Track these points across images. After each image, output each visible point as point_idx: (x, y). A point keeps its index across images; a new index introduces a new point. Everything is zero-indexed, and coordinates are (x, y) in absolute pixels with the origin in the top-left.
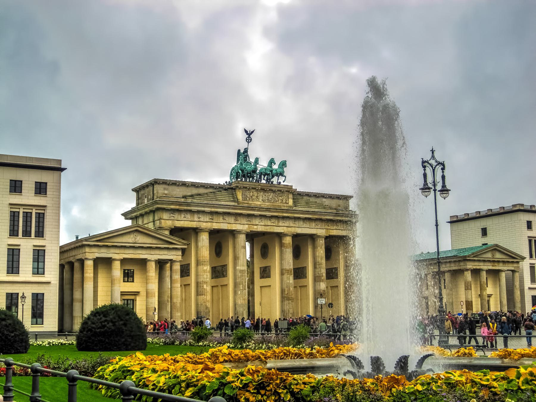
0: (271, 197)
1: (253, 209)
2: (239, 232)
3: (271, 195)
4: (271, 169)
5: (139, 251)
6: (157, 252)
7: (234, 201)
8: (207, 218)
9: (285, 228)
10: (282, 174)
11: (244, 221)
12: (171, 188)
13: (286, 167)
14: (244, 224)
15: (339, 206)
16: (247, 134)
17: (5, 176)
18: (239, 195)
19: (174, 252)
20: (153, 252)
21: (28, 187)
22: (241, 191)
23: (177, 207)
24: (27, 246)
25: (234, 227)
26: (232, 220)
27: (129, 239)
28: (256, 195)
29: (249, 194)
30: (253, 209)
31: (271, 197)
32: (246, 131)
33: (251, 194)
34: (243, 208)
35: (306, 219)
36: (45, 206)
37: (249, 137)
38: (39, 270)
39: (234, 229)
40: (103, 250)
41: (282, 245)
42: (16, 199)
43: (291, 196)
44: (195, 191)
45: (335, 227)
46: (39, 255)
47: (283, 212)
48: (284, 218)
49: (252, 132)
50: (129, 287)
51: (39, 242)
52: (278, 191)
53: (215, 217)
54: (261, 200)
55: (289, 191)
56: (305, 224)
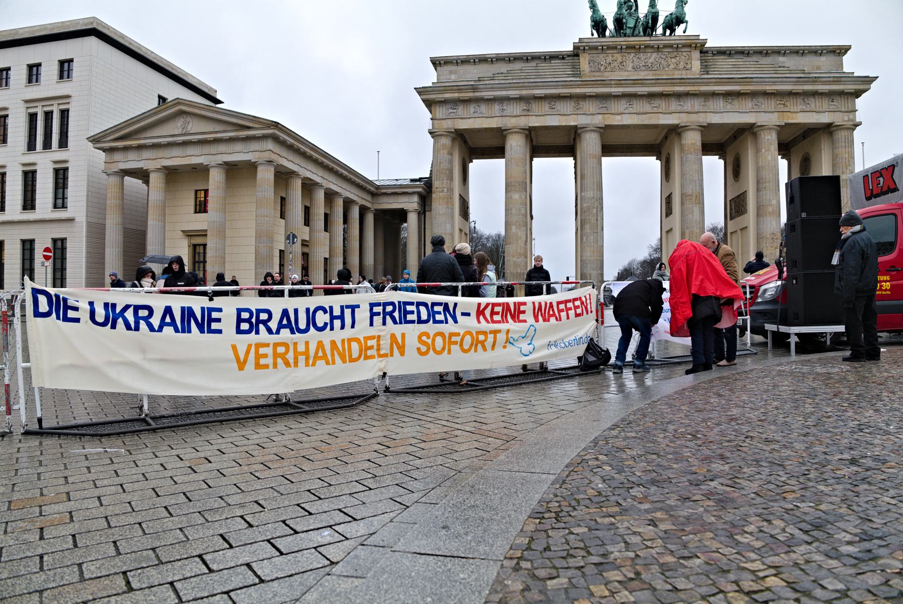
0: (652, 60)
1: (603, 83)
3: (652, 57)
4: (653, 11)
5: (191, 150)
6: (222, 148)
7: (574, 75)
8: (516, 109)
9: (684, 115)
11: (590, 106)
12: (462, 69)
14: (593, 115)
15: (818, 68)
17: (16, 61)
18: (584, 61)
19: (255, 146)
20: (213, 149)
21: (49, 71)
22: (586, 55)
23: (456, 95)
26: (566, 107)
27: (174, 129)
28: (620, 60)
29: (601, 58)
31: (652, 60)
33: (610, 59)
35: (728, 95)
36: (68, 97)
38: (60, 201)
40: (132, 155)
41: (682, 147)
43: (696, 55)
44: (504, 68)
45: (800, 108)
46: (61, 176)
47: (673, 84)
48: (679, 96)
51: (61, 155)
52: (665, 46)
53: (535, 107)
54: (630, 68)
55: (690, 46)
56: (729, 106)
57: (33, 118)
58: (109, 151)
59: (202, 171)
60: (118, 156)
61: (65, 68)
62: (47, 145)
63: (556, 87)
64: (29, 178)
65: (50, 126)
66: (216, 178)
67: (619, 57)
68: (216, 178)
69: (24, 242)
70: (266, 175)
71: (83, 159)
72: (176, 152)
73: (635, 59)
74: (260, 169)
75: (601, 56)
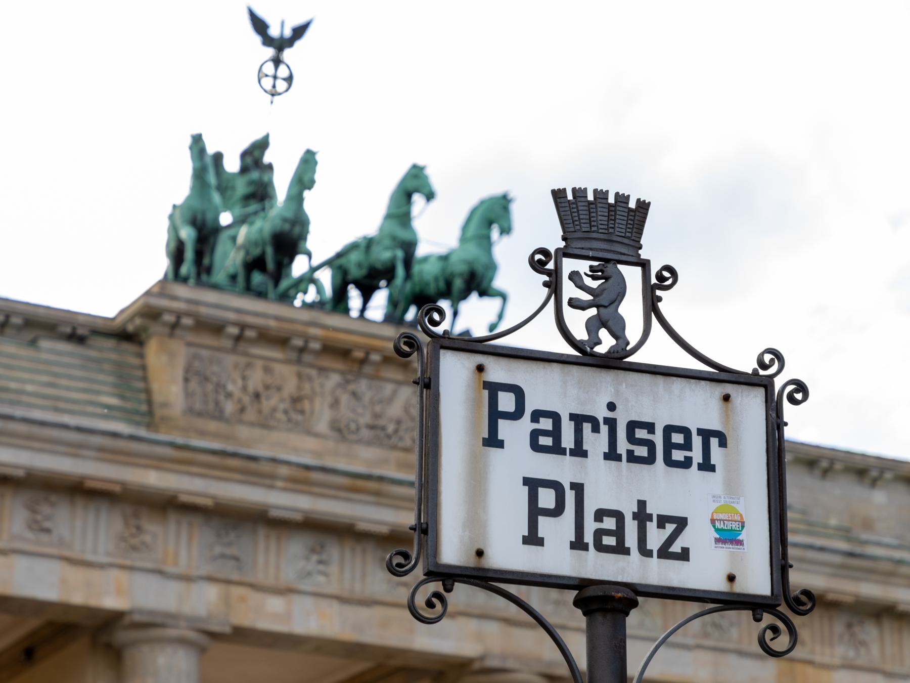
0: (395, 410)
1: (250, 467)
2: (149, 625)
4: (403, 234)
7: (128, 415)
10: (477, 282)
13: (506, 230)
14: (187, 579)
16: (268, 41)
25: (109, 593)
26: (92, 531)
28: (290, 386)
30: (250, 467)
32: (260, 26)
34: (184, 457)
37: (277, 61)
39: (111, 602)
49: (299, 32)
54: (322, 425)
63: (75, 450)
67: (287, 375)
73: (345, 398)
75: (230, 360)
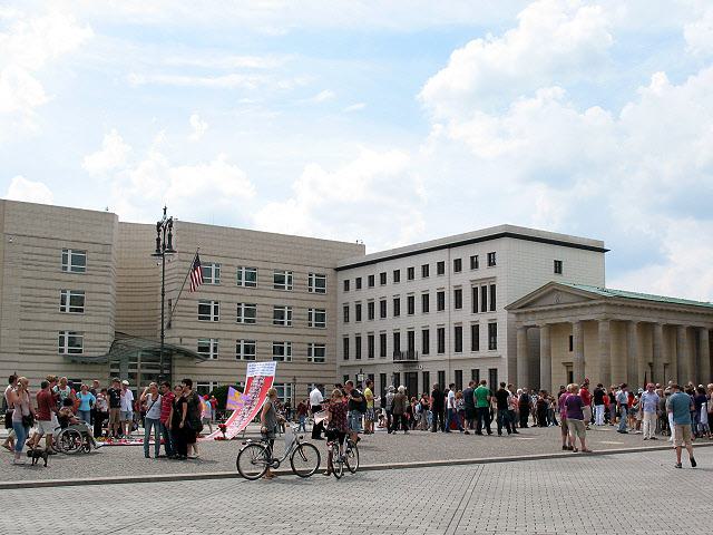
19: (597, 310)
21: (483, 261)
24: (483, 320)
27: (552, 299)
38: (493, 346)
42: (477, 274)
46: (493, 328)
50: (572, 357)
57: (475, 290)
58: (518, 314)
59: (568, 325)
60: (522, 317)
61: (491, 262)
62: (484, 309)
64: (475, 330)
65: (485, 297)
66: (576, 331)
68: (576, 331)
69: (473, 371)
70: (603, 328)
71: (502, 317)
72: (553, 314)
74: (600, 324)
